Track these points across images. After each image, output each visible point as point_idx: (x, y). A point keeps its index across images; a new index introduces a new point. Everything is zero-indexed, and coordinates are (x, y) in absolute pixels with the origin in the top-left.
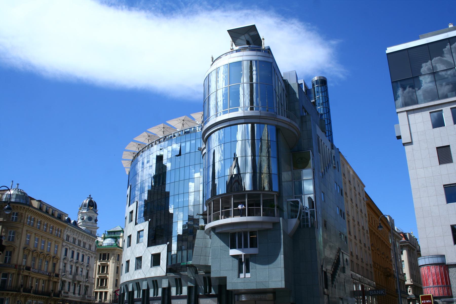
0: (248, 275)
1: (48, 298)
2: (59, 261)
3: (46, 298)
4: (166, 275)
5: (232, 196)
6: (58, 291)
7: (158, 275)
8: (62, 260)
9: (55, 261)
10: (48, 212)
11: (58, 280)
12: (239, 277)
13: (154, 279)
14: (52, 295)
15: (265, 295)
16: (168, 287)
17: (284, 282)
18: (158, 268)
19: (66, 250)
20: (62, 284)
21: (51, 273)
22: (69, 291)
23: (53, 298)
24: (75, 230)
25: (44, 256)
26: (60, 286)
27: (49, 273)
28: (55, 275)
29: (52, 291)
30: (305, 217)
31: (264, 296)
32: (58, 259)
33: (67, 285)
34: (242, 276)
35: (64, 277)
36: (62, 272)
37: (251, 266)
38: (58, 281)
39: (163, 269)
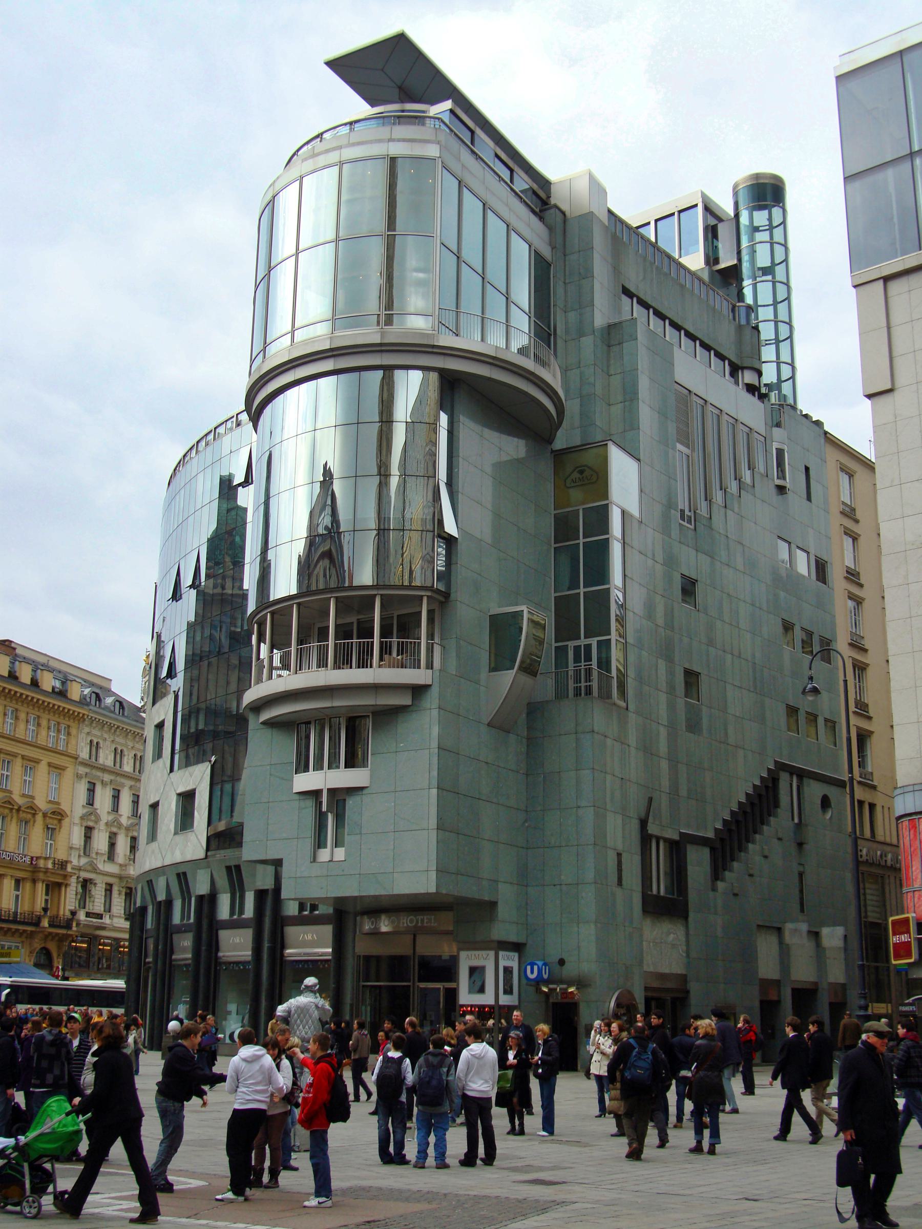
0: (340, 854)
1: (32, 932)
2: (66, 822)
3: (24, 931)
4: (207, 856)
5: (295, 605)
6: (68, 914)
7: (189, 857)
8: (77, 820)
9: (53, 823)
10: (17, 674)
11: (65, 877)
12: (314, 859)
13: (181, 870)
14: (45, 923)
15: (429, 917)
16: (209, 892)
17: (433, 875)
18: (191, 836)
19: (91, 791)
20: (80, 890)
21: (38, 858)
22: (109, 909)
23: (50, 933)
24: (118, 727)
25: (11, 807)
26: (76, 895)
27: (32, 858)
28: (54, 864)
29: (45, 910)
30: (583, 663)
31: (425, 921)
32: (62, 816)
33: (98, 893)
34: (324, 855)
35: (85, 870)
36: (79, 856)
37: (348, 824)
38: (66, 882)
39: (199, 837)
